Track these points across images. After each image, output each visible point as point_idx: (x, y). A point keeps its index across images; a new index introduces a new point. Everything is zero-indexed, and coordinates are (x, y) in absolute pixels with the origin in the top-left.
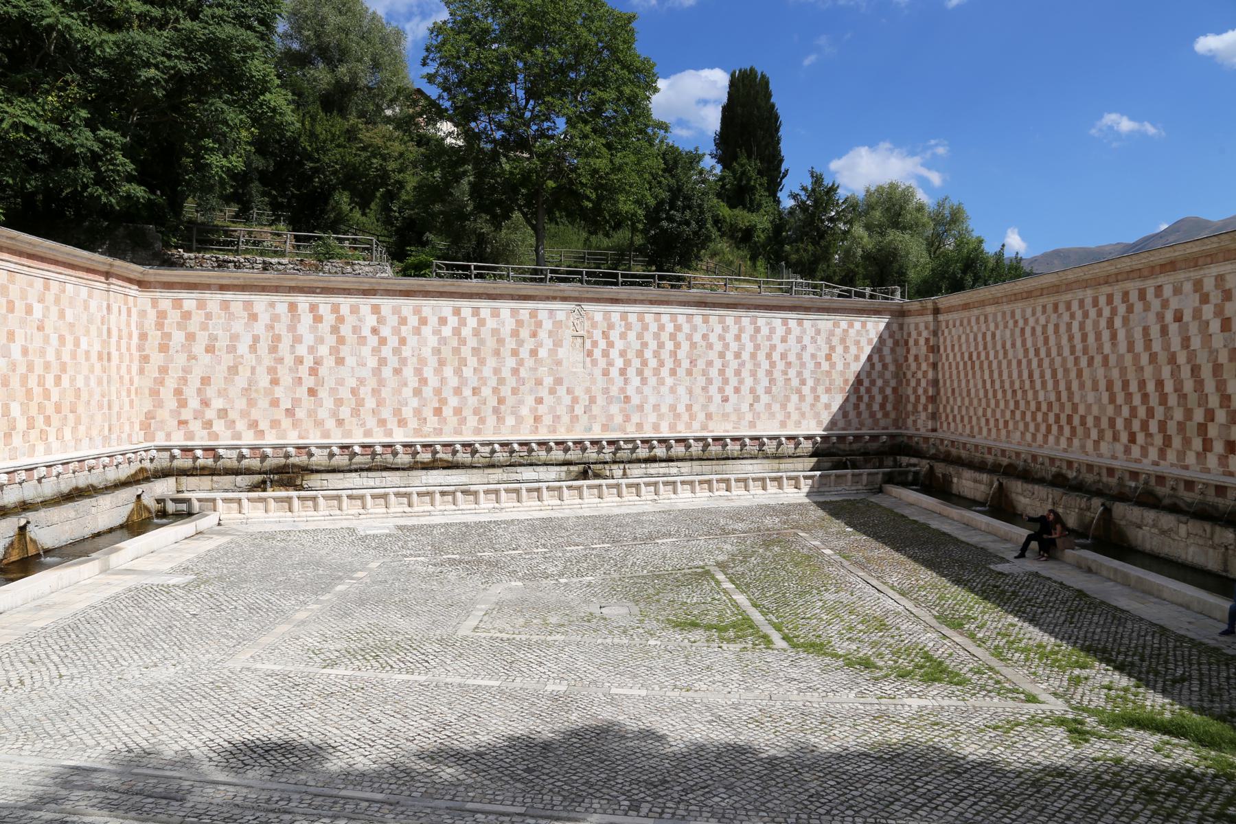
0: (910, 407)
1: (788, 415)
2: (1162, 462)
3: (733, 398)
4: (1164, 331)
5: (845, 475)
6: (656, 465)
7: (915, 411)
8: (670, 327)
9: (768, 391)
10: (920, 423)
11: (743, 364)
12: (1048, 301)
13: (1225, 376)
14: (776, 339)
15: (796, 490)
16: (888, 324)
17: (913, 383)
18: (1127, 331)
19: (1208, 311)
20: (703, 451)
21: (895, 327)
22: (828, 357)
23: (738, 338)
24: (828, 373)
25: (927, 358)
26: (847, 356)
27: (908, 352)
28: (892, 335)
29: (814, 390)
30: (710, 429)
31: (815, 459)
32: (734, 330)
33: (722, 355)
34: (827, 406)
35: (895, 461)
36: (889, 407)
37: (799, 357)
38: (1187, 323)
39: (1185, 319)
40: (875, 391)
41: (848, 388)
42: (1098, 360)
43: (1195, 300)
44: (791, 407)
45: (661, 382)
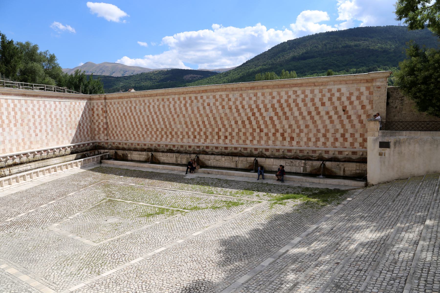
0: (96, 132)
1: (59, 139)
2: (205, 143)
3: (39, 134)
4: (204, 108)
5: (90, 159)
6: (24, 165)
8: (12, 105)
9: (51, 130)
10: (101, 138)
11: (41, 120)
12: (160, 98)
13: (224, 120)
14: (52, 110)
15: (77, 167)
16: (86, 103)
18: (192, 108)
19: (218, 104)
20: (34, 157)
21: (88, 104)
22: (70, 116)
23: (39, 109)
24: (70, 121)
25: (102, 115)
26: (76, 115)
27: (94, 112)
28: (88, 107)
29: (66, 128)
30: (32, 148)
31: (75, 155)
32: (37, 106)
33: (33, 117)
34: (71, 134)
35: (98, 152)
36: (89, 133)
37: (61, 116)
38: (212, 106)
39: (211, 105)
40: (85, 127)
41: (77, 127)
42: (181, 116)
43: (214, 100)
44: (59, 136)
45: (11, 130)
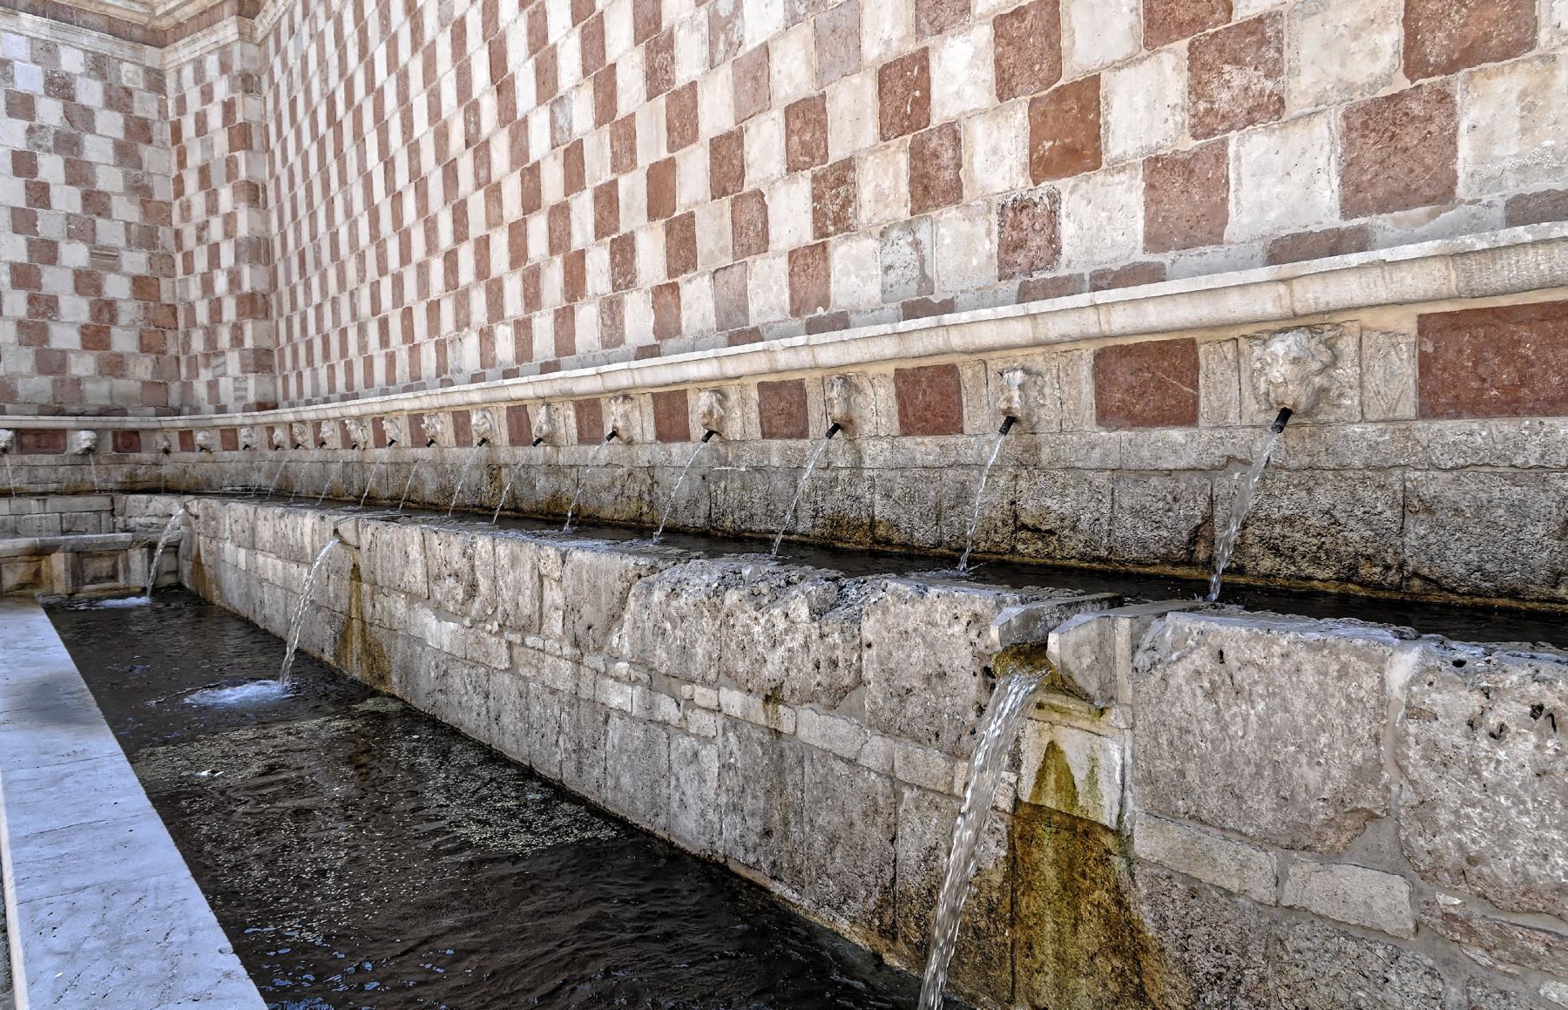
0: (198, 344)
7: (213, 351)
10: (226, 385)
17: (201, 264)
27: (182, 164)
36: (123, 341)
40: (55, 281)
